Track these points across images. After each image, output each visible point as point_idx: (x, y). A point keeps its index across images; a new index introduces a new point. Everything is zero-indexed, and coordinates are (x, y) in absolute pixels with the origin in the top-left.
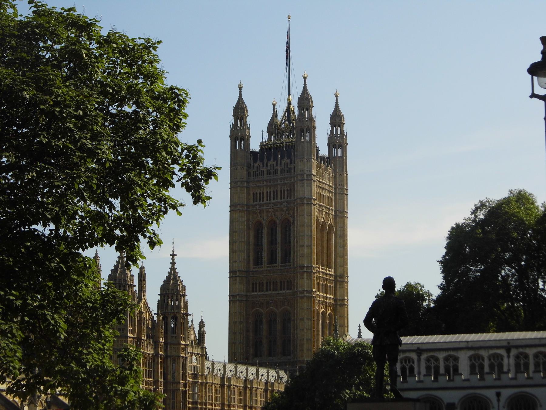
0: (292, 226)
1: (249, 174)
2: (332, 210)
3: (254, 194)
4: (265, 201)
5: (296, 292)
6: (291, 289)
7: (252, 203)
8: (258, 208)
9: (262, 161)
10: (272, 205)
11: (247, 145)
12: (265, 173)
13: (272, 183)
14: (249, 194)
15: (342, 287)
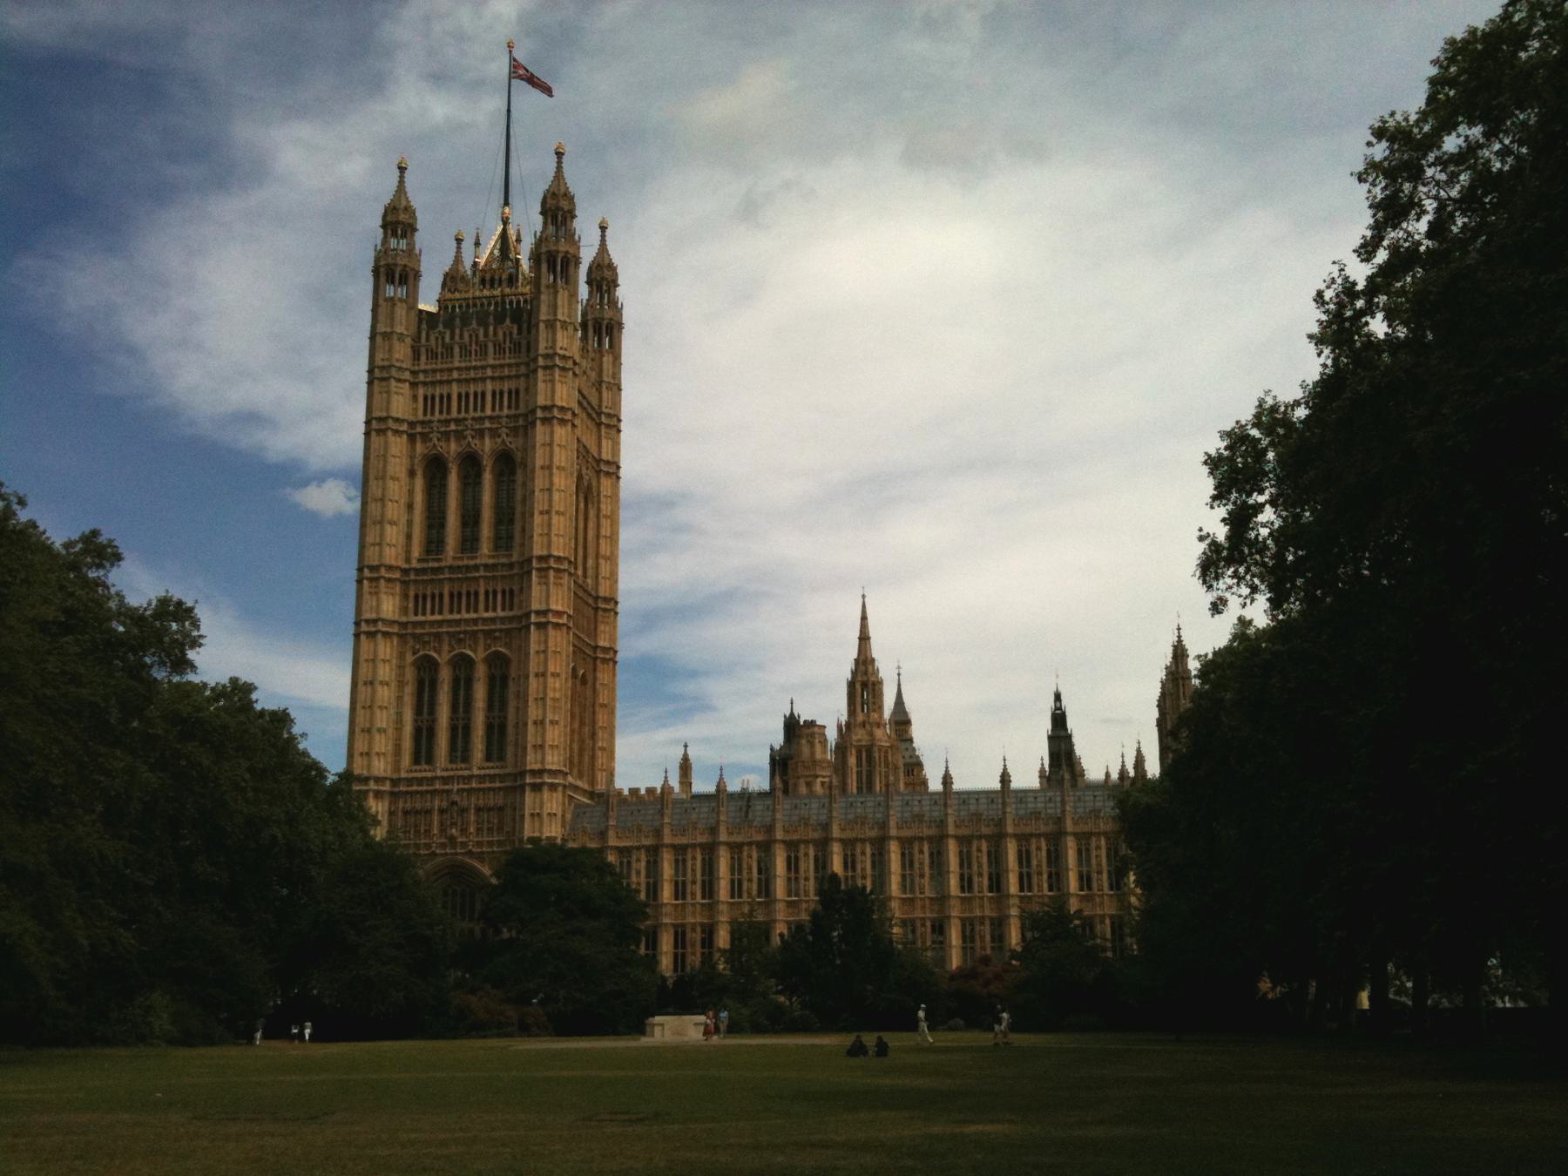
0: (519, 472)
1: (416, 355)
2: (593, 456)
3: (426, 398)
4: (454, 414)
5: (528, 615)
6: (511, 609)
7: (421, 417)
8: (435, 429)
9: (449, 324)
10: (470, 421)
11: (413, 297)
12: (457, 350)
13: (472, 374)
14: (415, 398)
15: (608, 623)
